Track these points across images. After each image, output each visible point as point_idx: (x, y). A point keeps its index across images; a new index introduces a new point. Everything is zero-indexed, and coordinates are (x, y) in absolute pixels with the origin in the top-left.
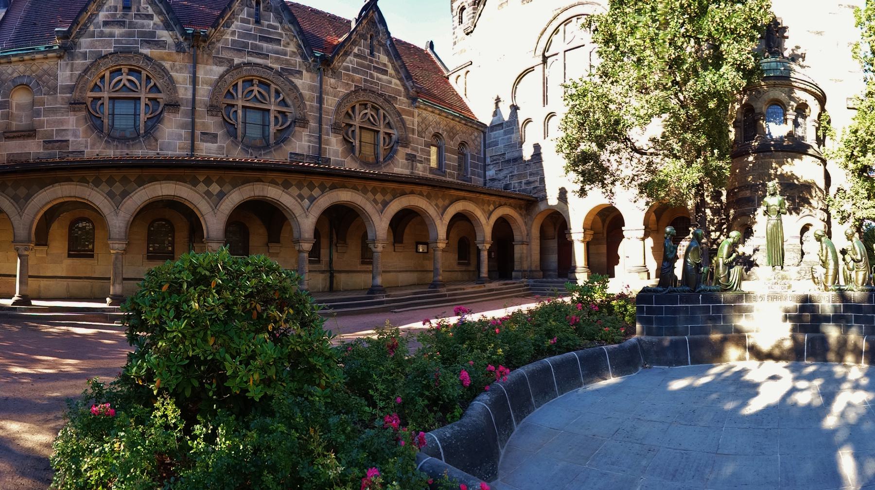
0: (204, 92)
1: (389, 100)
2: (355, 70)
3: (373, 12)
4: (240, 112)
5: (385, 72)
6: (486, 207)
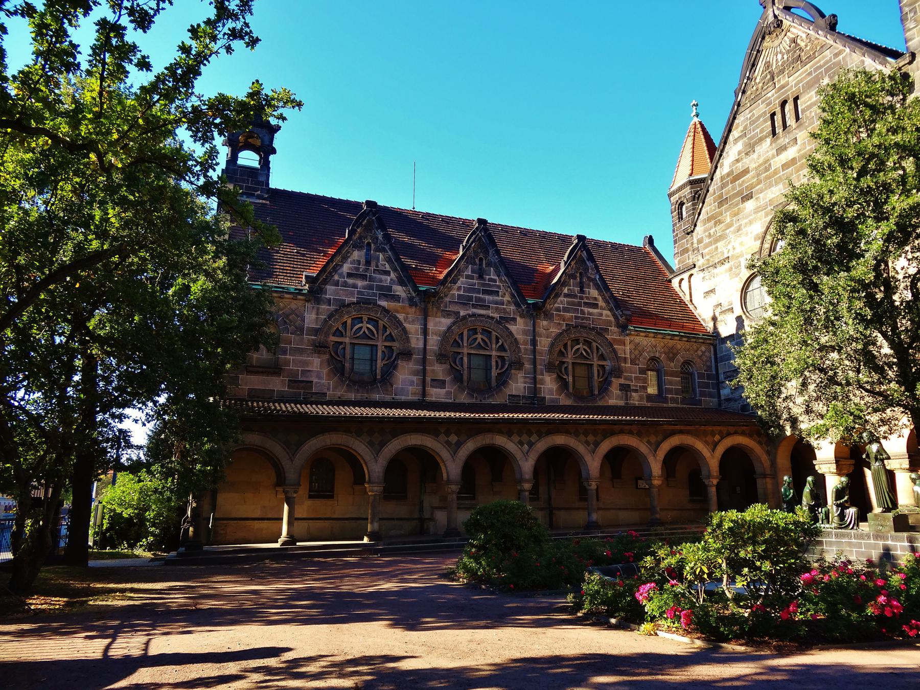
0: (434, 341)
1: (601, 332)
2: (566, 310)
3: (582, 251)
4: (465, 359)
5: (595, 306)
6: (709, 439)
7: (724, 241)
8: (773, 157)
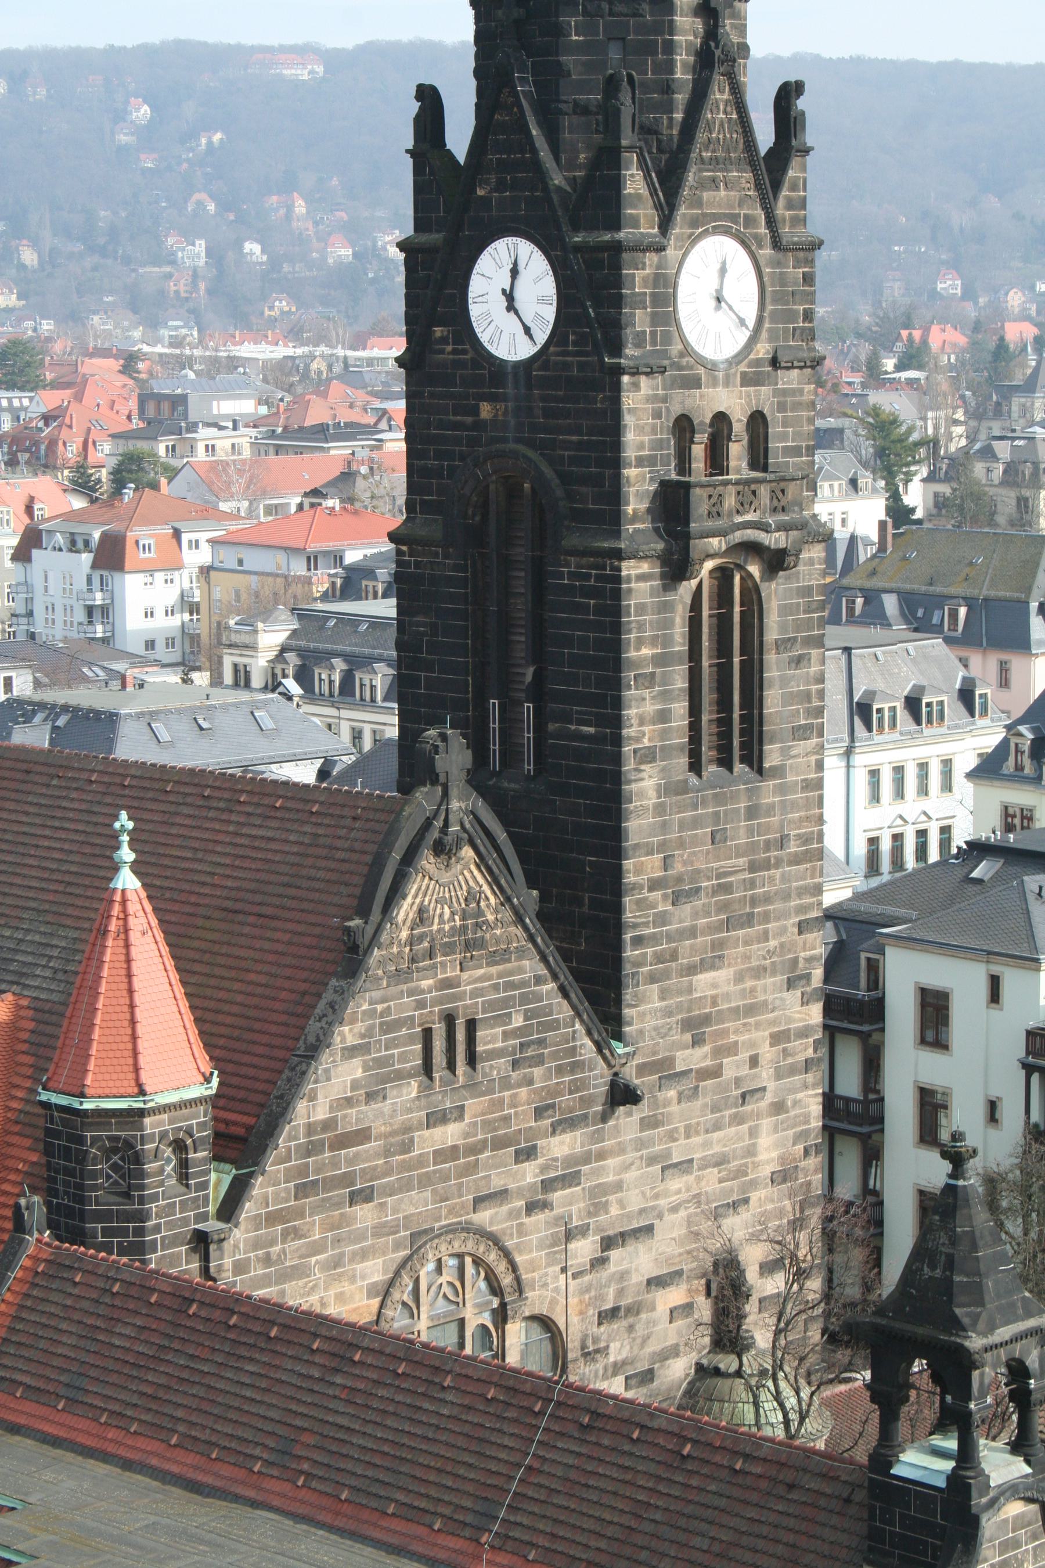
7: (301, 1283)
8: (419, 1128)
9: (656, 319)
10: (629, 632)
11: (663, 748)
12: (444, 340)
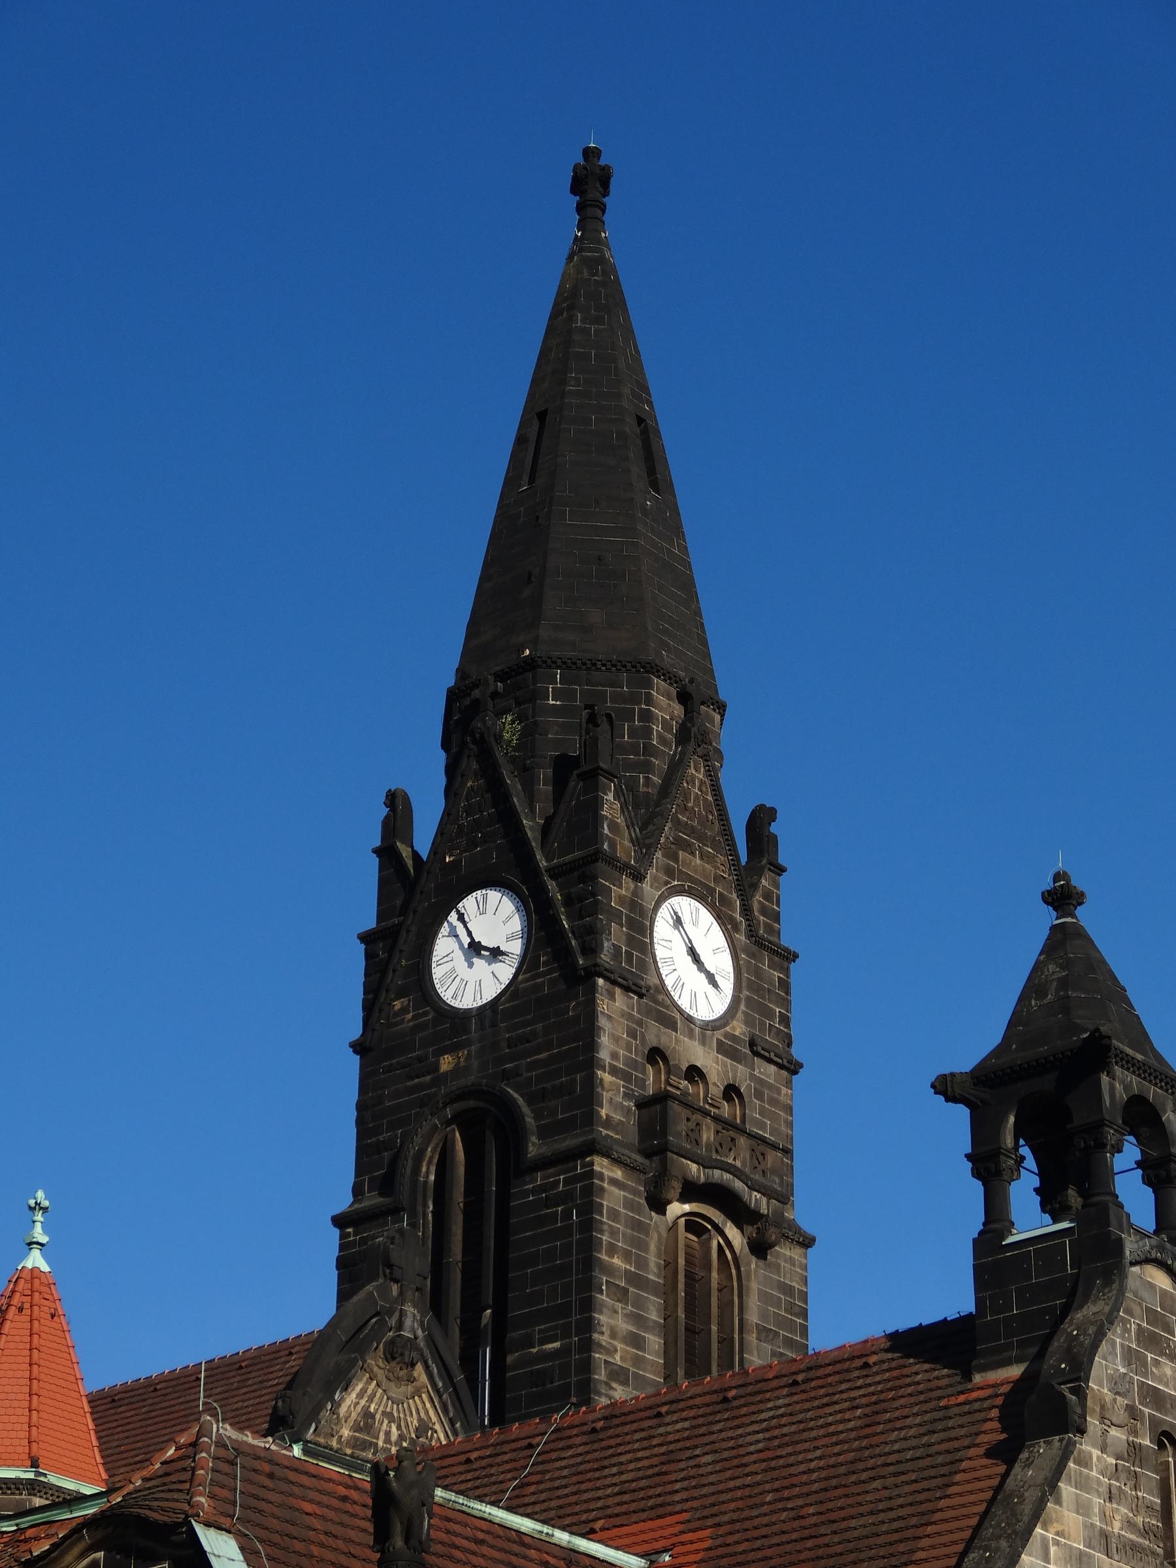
9: (630, 941)
10: (601, 1232)
11: (635, 1375)
12: (404, 1010)
